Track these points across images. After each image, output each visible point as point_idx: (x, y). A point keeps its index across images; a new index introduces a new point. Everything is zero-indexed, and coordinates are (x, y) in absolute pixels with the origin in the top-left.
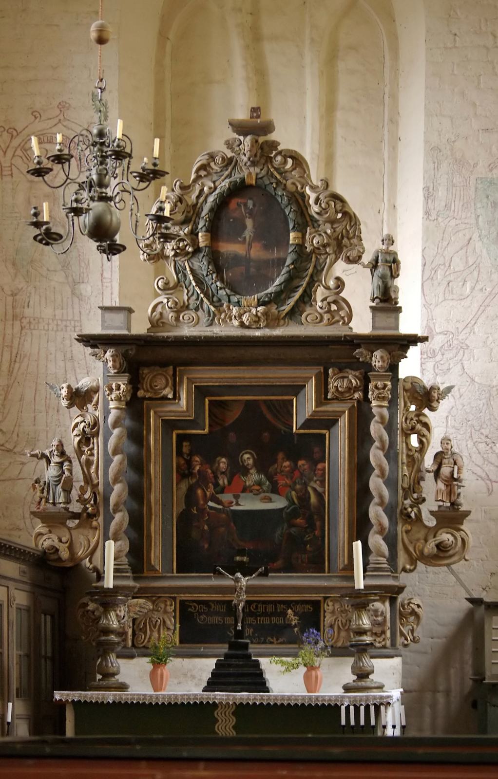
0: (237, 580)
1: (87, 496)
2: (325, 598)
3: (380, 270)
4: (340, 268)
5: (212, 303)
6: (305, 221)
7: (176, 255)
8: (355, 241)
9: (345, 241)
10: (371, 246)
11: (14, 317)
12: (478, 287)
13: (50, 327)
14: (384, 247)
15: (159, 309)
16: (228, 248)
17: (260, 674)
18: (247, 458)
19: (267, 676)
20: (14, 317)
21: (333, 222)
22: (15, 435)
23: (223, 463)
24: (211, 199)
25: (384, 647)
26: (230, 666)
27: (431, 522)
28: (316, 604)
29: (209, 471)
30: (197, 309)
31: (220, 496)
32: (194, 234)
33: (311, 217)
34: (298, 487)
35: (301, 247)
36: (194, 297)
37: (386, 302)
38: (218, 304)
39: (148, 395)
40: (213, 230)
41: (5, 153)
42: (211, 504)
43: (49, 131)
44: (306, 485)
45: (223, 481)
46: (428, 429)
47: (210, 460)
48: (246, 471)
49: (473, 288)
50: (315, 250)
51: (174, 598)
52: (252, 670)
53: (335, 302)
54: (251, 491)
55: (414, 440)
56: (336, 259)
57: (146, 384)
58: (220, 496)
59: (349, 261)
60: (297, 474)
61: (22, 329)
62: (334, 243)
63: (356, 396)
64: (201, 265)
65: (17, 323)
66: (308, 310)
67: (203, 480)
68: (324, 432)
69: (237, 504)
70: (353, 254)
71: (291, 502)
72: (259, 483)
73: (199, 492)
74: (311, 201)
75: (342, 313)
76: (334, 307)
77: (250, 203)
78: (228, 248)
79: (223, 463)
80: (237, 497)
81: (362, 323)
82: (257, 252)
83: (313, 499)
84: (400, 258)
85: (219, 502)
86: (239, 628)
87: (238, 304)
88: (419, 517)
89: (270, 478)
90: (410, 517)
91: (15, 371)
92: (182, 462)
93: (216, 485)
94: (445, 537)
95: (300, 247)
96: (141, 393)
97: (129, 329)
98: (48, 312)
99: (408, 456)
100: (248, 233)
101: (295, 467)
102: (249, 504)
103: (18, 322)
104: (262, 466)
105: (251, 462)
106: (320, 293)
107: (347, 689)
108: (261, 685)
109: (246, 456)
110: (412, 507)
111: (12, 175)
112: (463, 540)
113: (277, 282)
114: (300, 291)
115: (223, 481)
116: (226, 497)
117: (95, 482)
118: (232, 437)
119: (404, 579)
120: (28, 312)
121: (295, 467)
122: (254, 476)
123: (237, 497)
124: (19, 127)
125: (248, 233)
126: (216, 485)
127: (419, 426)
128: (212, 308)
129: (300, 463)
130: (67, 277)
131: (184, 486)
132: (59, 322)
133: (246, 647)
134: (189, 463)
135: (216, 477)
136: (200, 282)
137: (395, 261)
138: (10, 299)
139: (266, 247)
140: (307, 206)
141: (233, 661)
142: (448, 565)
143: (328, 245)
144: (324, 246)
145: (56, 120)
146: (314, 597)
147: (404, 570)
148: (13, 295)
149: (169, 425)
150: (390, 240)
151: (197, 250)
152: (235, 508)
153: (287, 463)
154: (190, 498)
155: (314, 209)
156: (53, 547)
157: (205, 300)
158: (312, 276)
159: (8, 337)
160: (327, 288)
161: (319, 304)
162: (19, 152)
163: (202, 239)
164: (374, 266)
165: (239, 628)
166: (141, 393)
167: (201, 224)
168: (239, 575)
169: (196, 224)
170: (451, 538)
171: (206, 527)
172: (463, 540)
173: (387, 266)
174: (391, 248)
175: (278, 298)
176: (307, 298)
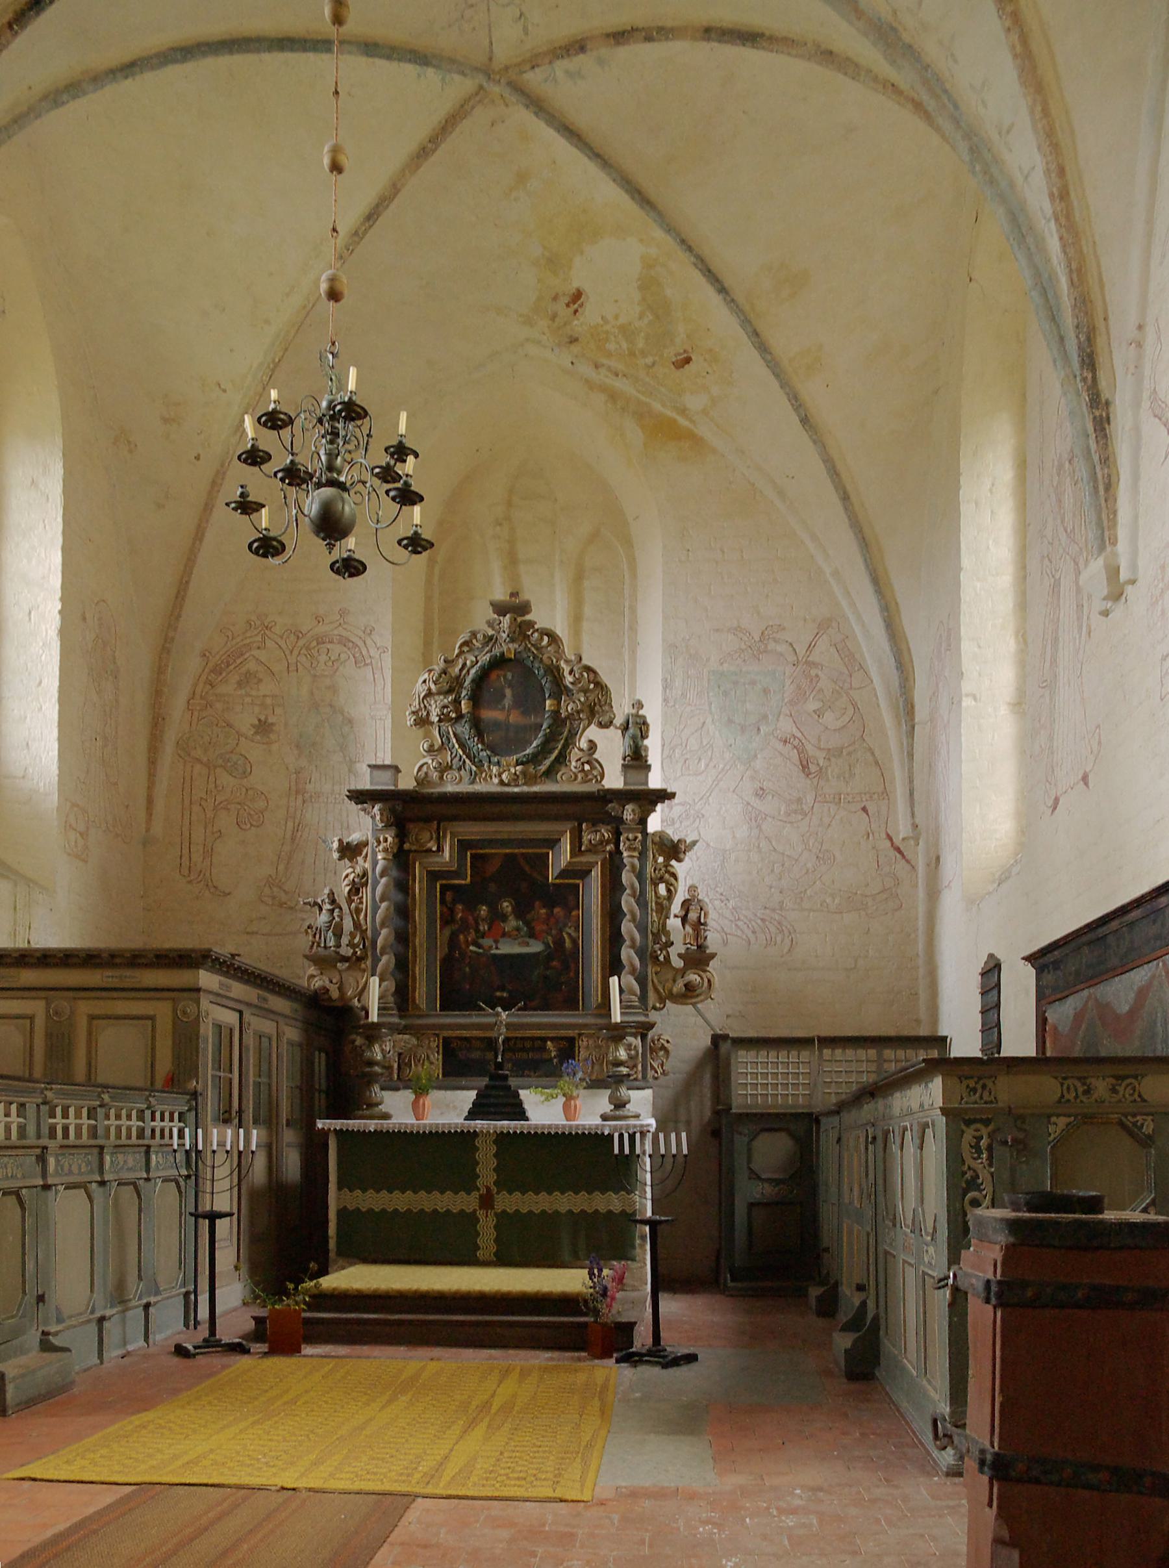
0: (498, 1014)
1: (356, 941)
2: (580, 1035)
3: (631, 731)
4: (593, 732)
5: (474, 763)
6: (559, 690)
7: (440, 721)
8: (606, 708)
9: (597, 708)
10: (621, 710)
11: (297, 792)
12: (712, 764)
14: (634, 711)
15: (425, 769)
16: (489, 714)
17: (520, 1104)
18: (506, 906)
19: (526, 1106)
20: (297, 792)
21: (585, 691)
23: (484, 910)
24: (473, 671)
25: (636, 1079)
26: (490, 1096)
27: (677, 963)
28: (571, 1041)
29: (470, 918)
30: (459, 769)
31: (481, 941)
32: (457, 702)
33: (566, 687)
34: (554, 932)
35: (556, 713)
36: (458, 758)
37: (636, 760)
38: (479, 765)
40: (476, 699)
42: (472, 948)
44: (561, 931)
45: (484, 927)
46: (676, 879)
47: (471, 907)
48: (504, 918)
49: (707, 765)
50: (568, 717)
51: (437, 1035)
52: (512, 1101)
53: (588, 762)
54: (510, 936)
55: (662, 889)
56: (589, 725)
57: (412, 838)
58: (481, 941)
59: (601, 725)
60: (552, 920)
61: (304, 802)
62: (587, 709)
63: (608, 848)
64: (464, 729)
65: (300, 797)
66: (563, 770)
67: (465, 927)
68: (577, 881)
69: (497, 948)
70: (605, 719)
71: (547, 945)
72: (518, 929)
73: (461, 937)
74: (566, 673)
75: (595, 773)
76: (587, 767)
77: (509, 675)
78: (489, 714)
79: (484, 910)
80: (496, 942)
81: (614, 780)
82: (515, 718)
83: (568, 944)
84: (649, 720)
85: (480, 946)
86: (500, 1060)
87: (498, 763)
88: (667, 958)
89: (527, 923)
90: (657, 957)
92: (445, 910)
93: (477, 930)
94: (693, 977)
95: (556, 713)
96: (406, 846)
97: (396, 785)
99: (656, 903)
100: (507, 702)
101: (550, 915)
102: (507, 948)
104: (521, 912)
105: (510, 909)
106: (575, 754)
107: (604, 1118)
108: (521, 1115)
109: (505, 904)
110: (661, 950)
112: (709, 981)
113: (534, 744)
114: (556, 752)
115: (484, 927)
116: (487, 942)
118: (493, 887)
119: (654, 1016)
120: (309, 787)
121: (550, 915)
122: (512, 923)
123: (496, 942)
124: (304, 629)
125: (507, 702)
126: (477, 930)
127: (667, 876)
128: (474, 768)
129: (556, 910)
130: (345, 757)
131: (447, 932)
133: (505, 1078)
134: (452, 911)
135: (477, 924)
136: (462, 745)
137: (645, 723)
139: (526, 713)
140: (562, 677)
141: (494, 1092)
142: (694, 1005)
143: (582, 711)
144: (578, 712)
146: (570, 1033)
147: (654, 1008)
148: (297, 773)
149: (433, 876)
150: (639, 705)
151: (460, 716)
152: (494, 951)
153: (543, 911)
154: (453, 942)
155: (569, 679)
156: (324, 988)
157: (467, 761)
158: (566, 740)
159: (292, 810)
160: (581, 750)
161: (574, 764)
163: (465, 706)
164: (625, 728)
165: (500, 1060)
166: (406, 846)
167: (464, 693)
168: (499, 1009)
169: (459, 694)
170: (699, 979)
171: (467, 969)
172: (709, 981)
173: (637, 728)
174: (641, 712)
175: (535, 759)
176: (562, 759)
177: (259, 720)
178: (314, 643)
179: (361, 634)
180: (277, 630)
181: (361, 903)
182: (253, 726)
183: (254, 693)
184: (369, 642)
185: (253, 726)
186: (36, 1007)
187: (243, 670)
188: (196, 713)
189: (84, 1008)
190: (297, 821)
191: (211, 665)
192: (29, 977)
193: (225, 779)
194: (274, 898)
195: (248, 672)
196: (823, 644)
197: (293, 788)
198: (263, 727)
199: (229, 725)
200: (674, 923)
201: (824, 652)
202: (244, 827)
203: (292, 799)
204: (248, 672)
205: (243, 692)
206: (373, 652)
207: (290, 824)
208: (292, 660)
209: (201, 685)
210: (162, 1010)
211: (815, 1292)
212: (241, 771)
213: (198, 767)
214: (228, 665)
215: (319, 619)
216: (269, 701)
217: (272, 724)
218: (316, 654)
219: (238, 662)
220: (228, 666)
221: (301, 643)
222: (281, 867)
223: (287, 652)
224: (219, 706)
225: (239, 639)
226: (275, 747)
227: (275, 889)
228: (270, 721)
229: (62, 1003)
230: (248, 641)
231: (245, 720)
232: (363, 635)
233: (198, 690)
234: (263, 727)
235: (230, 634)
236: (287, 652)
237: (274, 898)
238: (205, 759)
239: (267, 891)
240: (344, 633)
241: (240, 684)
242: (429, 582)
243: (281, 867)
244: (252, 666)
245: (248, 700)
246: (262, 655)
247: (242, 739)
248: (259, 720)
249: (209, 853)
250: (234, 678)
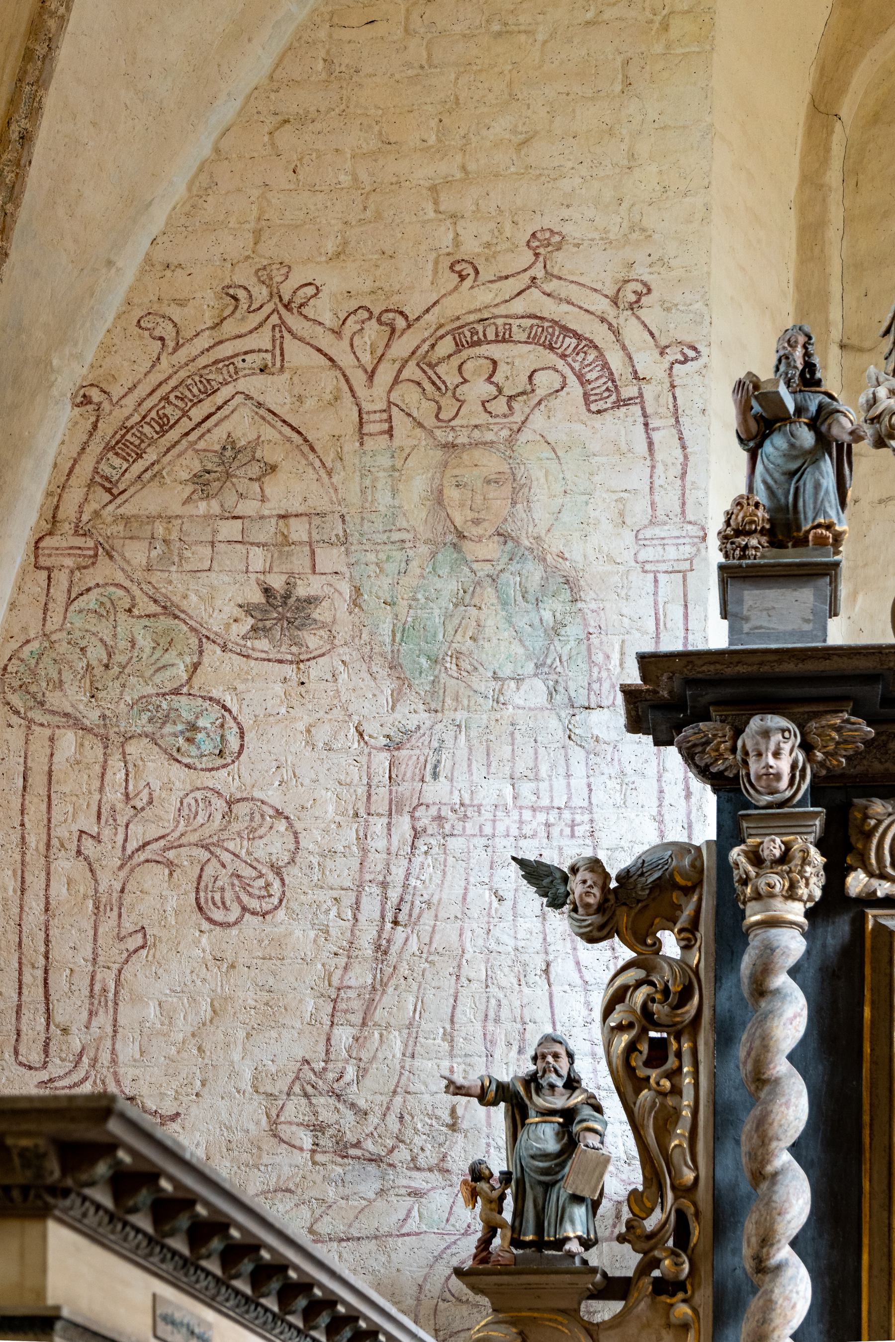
11: (394, 807)
13: (501, 828)
20: (394, 807)
22: (392, 1119)
39: (883, 889)
41: (371, 376)
43: (502, 310)
65: (403, 825)
91: (394, 950)
96: (857, 882)
98: (493, 790)
103: (407, 818)
111: (390, 432)
117: (689, 1176)
132: (527, 815)
138: (382, 760)
145: (525, 278)
148: (393, 746)
159: (376, 861)
162: (411, 371)
166: (857, 882)
177: (267, 591)
178: (446, 346)
179: (602, 305)
180: (324, 310)
181: (676, 1091)
182: (248, 609)
183: (248, 507)
184: (632, 332)
185: (248, 609)
187: (218, 435)
188: (62, 579)
190: (394, 895)
191: (106, 429)
193: (157, 771)
194: (318, 1128)
195: (230, 442)
197: (381, 795)
198: (281, 612)
199: (170, 610)
202: (218, 915)
203: (378, 825)
204: (230, 442)
205: (215, 507)
206: (648, 362)
207: (371, 907)
208: (374, 398)
209: (74, 496)
212: (208, 747)
213: (68, 740)
214: (164, 426)
215: (463, 269)
216: (299, 530)
217: (311, 601)
218: (452, 379)
219: (197, 414)
220: (163, 432)
221: (402, 347)
222: (343, 1036)
223: (358, 378)
224: (137, 554)
225: (204, 342)
226: (316, 670)
227: (320, 1100)
228: (301, 591)
230: (226, 350)
231: (221, 595)
232: (611, 313)
233: (68, 510)
234: (281, 612)
235: (168, 331)
236: (358, 378)
237: (318, 1128)
238: (92, 716)
239: (295, 1109)
240: (551, 309)
241: (203, 484)
242: (811, 180)
243: (343, 1036)
244: (241, 425)
245: (230, 530)
246: (274, 391)
247: (212, 653)
248: (267, 591)
250: (187, 465)
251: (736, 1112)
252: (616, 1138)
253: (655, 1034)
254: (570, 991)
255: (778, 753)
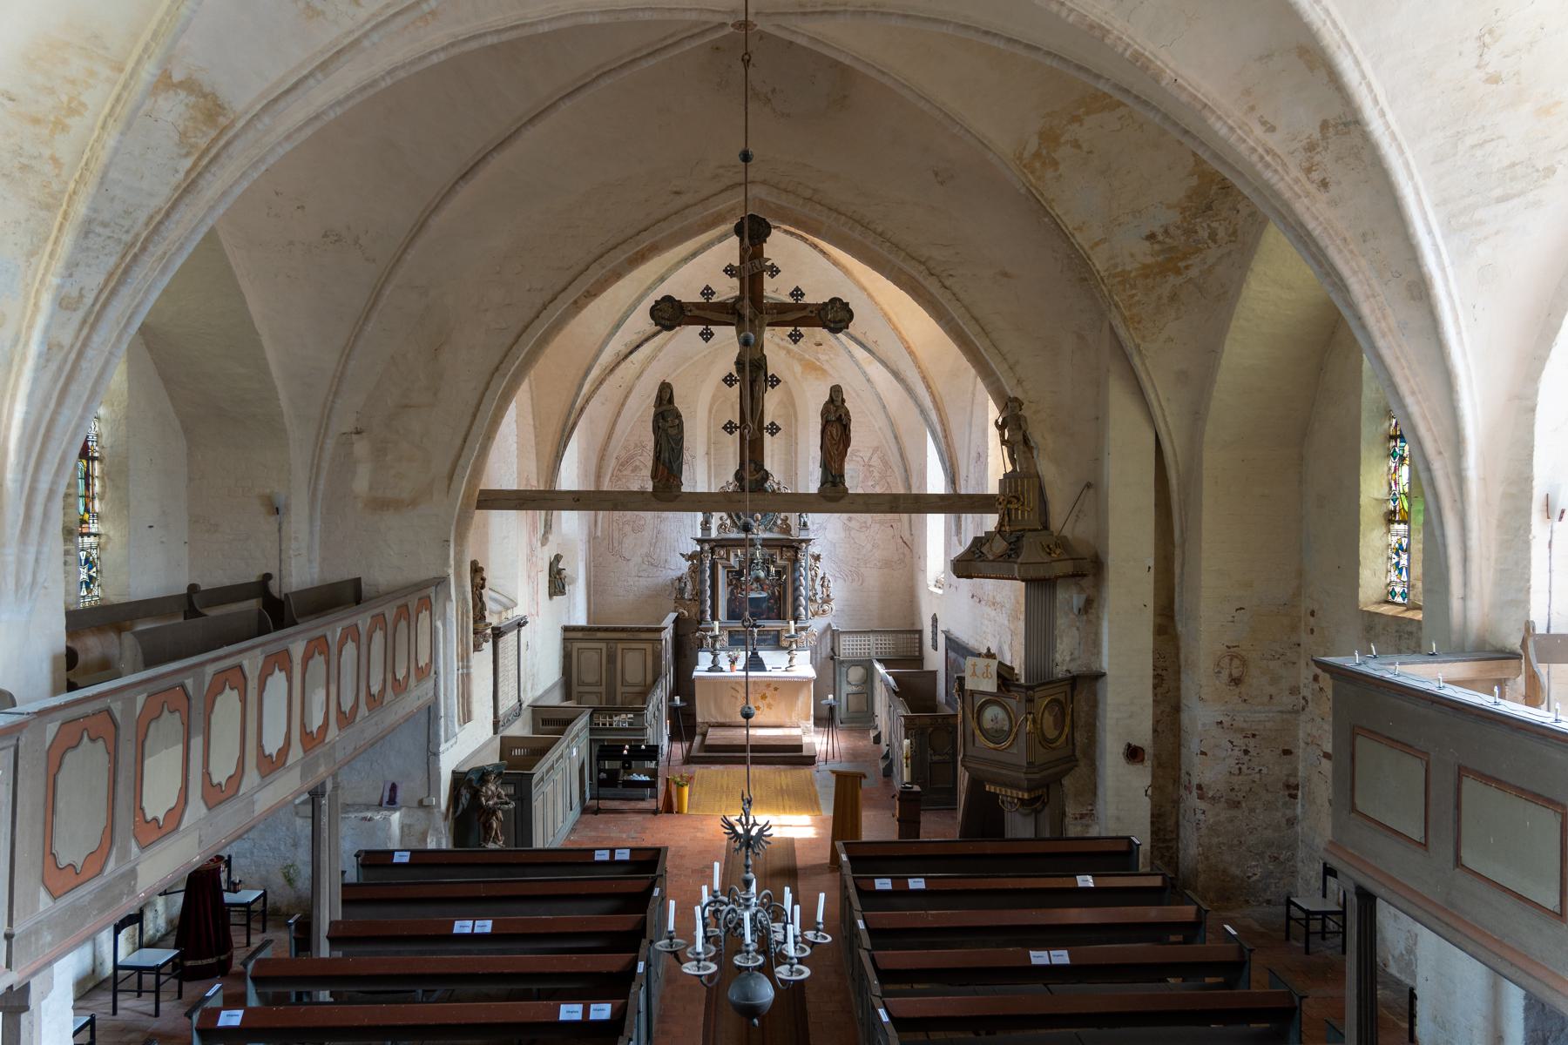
81: (795, 534)
102: (753, 595)
154: (732, 592)
186: (603, 645)
189: (620, 646)
192: (600, 635)
196: (875, 458)
200: (818, 587)
201: (875, 461)
210: (648, 646)
211: (872, 734)
229: (612, 644)
249: (620, 543)
251: (702, 582)
252: (689, 587)
253: (696, 571)
254: (685, 566)
255: (707, 547)
